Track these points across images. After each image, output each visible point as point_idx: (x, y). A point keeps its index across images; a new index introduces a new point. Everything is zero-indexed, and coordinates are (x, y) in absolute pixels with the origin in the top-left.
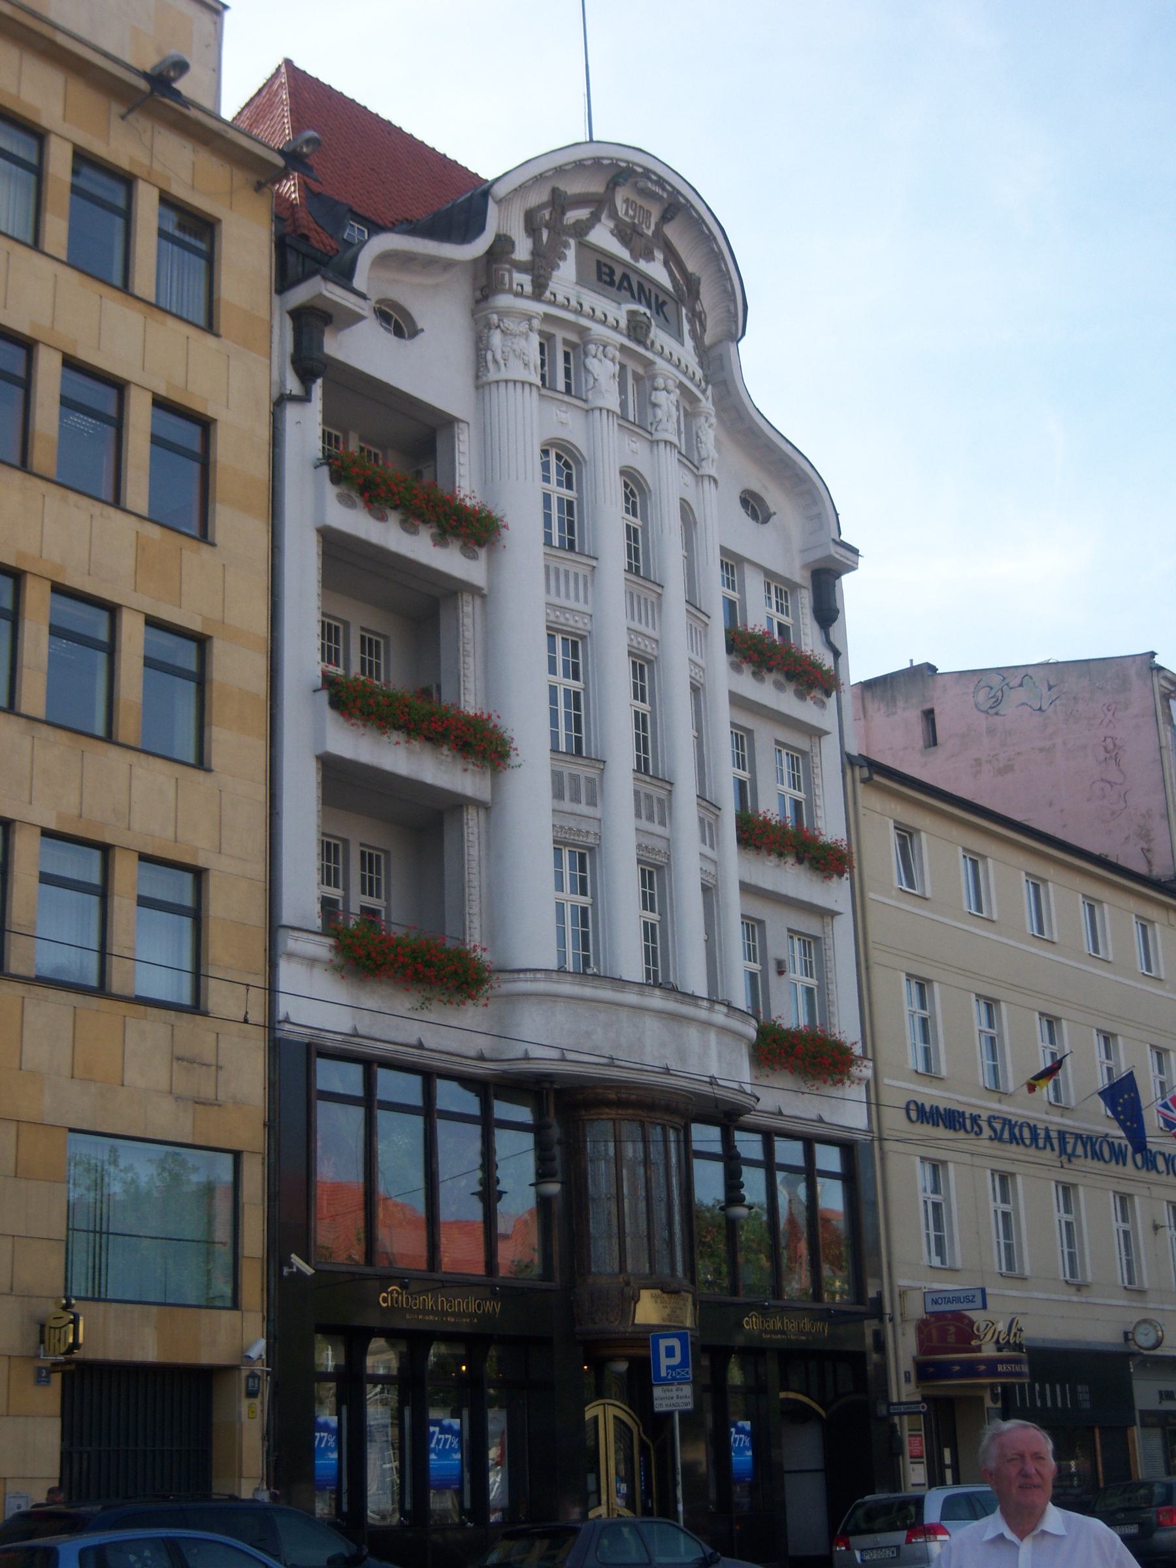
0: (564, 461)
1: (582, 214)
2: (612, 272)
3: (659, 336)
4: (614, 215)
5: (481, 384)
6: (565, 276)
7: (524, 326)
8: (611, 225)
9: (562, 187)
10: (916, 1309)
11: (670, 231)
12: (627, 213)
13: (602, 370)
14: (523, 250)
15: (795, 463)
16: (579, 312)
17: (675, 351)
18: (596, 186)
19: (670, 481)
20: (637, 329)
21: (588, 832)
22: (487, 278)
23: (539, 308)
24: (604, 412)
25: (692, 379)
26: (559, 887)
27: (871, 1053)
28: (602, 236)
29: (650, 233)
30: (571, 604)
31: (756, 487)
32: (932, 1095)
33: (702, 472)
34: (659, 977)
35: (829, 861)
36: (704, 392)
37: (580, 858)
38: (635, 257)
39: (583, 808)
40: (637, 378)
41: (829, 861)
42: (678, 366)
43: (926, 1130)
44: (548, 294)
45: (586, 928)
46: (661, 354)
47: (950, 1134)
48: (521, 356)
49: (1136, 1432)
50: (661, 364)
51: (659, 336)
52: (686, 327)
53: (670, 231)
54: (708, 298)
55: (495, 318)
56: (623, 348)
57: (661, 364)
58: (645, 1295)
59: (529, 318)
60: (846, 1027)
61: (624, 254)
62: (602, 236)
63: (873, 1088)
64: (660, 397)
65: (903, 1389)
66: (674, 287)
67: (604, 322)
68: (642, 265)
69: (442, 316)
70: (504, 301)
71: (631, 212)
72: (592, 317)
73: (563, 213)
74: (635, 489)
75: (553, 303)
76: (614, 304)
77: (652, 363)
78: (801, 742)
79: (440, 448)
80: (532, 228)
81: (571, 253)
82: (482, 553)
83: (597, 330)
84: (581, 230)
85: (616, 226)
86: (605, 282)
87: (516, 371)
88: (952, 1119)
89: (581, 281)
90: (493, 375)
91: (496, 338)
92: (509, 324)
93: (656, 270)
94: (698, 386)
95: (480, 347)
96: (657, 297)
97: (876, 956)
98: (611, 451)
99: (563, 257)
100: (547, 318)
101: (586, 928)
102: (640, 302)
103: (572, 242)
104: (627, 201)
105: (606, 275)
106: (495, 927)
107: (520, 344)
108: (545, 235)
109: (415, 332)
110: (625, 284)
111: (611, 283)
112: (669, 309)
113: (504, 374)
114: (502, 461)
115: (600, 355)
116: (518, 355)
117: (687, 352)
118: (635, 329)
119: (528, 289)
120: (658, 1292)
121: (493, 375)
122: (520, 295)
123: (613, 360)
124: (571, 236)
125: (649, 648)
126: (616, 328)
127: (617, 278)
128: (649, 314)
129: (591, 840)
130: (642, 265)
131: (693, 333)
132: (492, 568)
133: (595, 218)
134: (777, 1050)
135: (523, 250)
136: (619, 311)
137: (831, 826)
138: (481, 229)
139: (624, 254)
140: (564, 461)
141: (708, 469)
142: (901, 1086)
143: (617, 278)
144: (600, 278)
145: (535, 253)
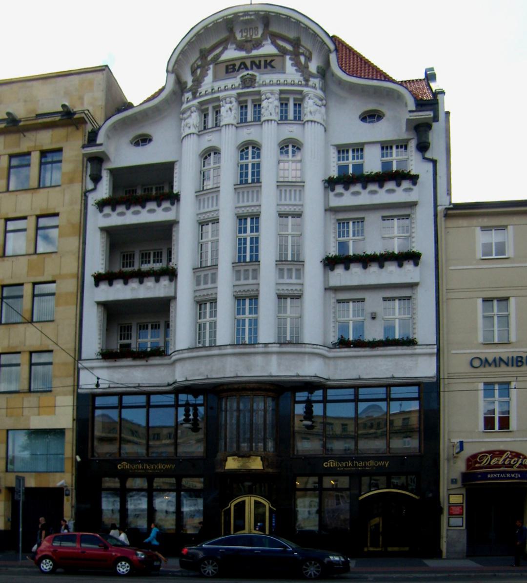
2: (234, 65)
3: (263, 77)
6: (208, 82)
7: (189, 113)
8: (234, 46)
9: (203, 47)
11: (274, 29)
12: (242, 37)
15: (380, 87)
16: (213, 92)
18: (224, 35)
20: (248, 82)
21: (212, 294)
23: (195, 102)
24: (224, 126)
25: (293, 85)
28: (231, 54)
29: (259, 36)
33: (305, 120)
36: (307, 85)
38: (249, 51)
42: (279, 85)
44: (198, 94)
46: (265, 85)
50: (263, 89)
56: (239, 95)
57: (263, 89)
58: (230, 459)
59: (189, 108)
61: (243, 54)
66: (279, 51)
67: (226, 90)
68: (255, 53)
70: (185, 106)
71: (244, 34)
72: (221, 91)
73: (206, 58)
76: (234, 79)
80: (193, 72)
81: (210, 73)
82: (174, 208)
83: (221, 95)
84: (215, 61)
85: (236, 45)
86: (230, 72)
87: (187, 131)
89: (216, 78)
93: (268, 49)
94: (301, 85)
96: (266, 61)
99: (207, 75)
100: (201, 104)
102: (252, 69)
103: (211, 66)
104: (241, 31)
105: (231, 68)
110: (242, 66)
111: (234, 70)
115: (224, 104)
117: (291, 74)
118: (244, 83)
120: (236, 457)
123: (231, 103)
124: (210, 64)
126: (233, 89)
127: (237, 67)
128: (250, 72)
129: (214, 296)
130: (255, 53)
131: (297, 64)
132: (178, 212)
133: (225, 49)
136: (236, 81)
139: (243, 54)
143: (237, 67)
144: (227, 72)
145: (193, 81)
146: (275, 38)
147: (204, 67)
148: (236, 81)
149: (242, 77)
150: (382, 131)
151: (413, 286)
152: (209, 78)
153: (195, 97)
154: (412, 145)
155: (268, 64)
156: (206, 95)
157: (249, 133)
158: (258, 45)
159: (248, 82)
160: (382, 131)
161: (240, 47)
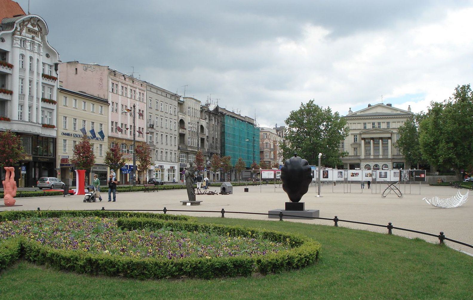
0: (23, 56)
1: (27, 23)
4: (31, 22)
5: (12, 47)
7: (18, 40)
10: (61, 158)
11: (38, 23)
13: (28, 44)
14: (19, 30)
16: (26, 37)
17: (38, 39)
19: (36, 57)
20: (33, 38)
22: (14, 34)
23: (20, 37)
26: (19, 110)
27: (57, 127)
30: (21, 100)
31: (48, 53)
32: (65, 132)
34: (30, 121)
35: (54, 102)
36: (41, 43)
37: (21, 106)
39: (22, 101)
40: (32, 43)
41: (54, 102)
43: (65, 136)
45: (21, 115)
47: (67, 136)
48: (18, 43)
49: (91, 174)
51: (36, 38)
52: (40, 35)
53: (38, 23)
54: (43, 30)
55: (14, 38)
56: (31, 41)
59: (19, 38)
60: (54, 124)
62: (30, 26)
63: (57, 131)
64: (35, 46)
65: (58, 167)
67: (29, 38)
68: (34, 28)
69: (8, 40)
70: (16, 36)
72: (27, 37)
74: (31, 58)
75: (22, 36)
77: (34, 42)
78: (51, 87)
79: (7, 54)
80: (20, 26)
81: (25, 29)
82: (11, 69)
84: (26, 25)
88: (68, 135)
90: (14, 46)
91: (15, 41)
92: (16, 39)
93: (36, 29)
95: (13, 42)
97: (59, 114)
98: (28, 54)
100: (21, 38)
101: (21, 115)
105: (30, 31)
106: (11, 116)
107: (17, 42)
108: (22, 26)
109: (4, 41)
112: (37, 34)
113: (15, 46)
114: (14, 58)
116: (17, 43)
119: (19, 34)
121: (14, 46)
122: (18, 35)
125: (32, 79)
126: (30, 38)
130: (34, 28)
131: (41, 36)
133: (28, 23)
134: (45, 126)
135: (19, 30)
136: (30, 36)
137: (54, 99)
138: (14, 28)
139: (32, 27)
140: (23, 56)
141: (41, 54)
142: (61, 130)
145: (20, 29)
146: (38, 26)
147: (23, 26)
148: (30, 36)
149: (32, 36)
150: (48, 61)
151: (53, 110)
152: (24, 31)
153: (20, 35)
154: (54, 67)
155: (35, 32)
156: (23, 36)
157: (31, 54)
158: (35, 27)
159: (33, 38)
160: (48, 61)
161: (32, 25)
